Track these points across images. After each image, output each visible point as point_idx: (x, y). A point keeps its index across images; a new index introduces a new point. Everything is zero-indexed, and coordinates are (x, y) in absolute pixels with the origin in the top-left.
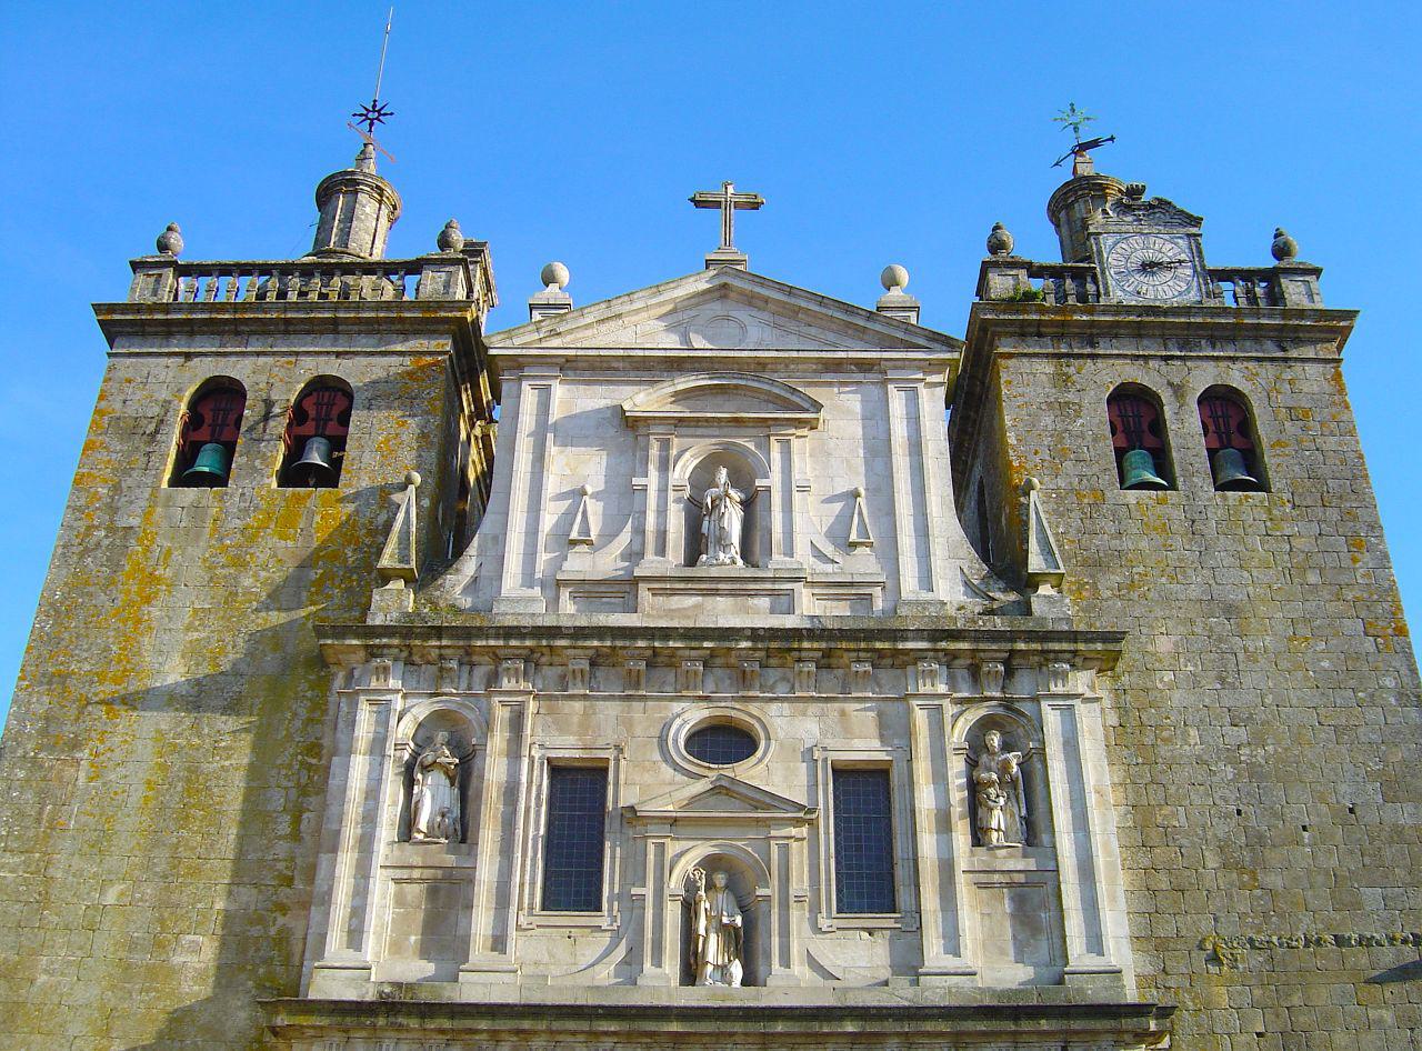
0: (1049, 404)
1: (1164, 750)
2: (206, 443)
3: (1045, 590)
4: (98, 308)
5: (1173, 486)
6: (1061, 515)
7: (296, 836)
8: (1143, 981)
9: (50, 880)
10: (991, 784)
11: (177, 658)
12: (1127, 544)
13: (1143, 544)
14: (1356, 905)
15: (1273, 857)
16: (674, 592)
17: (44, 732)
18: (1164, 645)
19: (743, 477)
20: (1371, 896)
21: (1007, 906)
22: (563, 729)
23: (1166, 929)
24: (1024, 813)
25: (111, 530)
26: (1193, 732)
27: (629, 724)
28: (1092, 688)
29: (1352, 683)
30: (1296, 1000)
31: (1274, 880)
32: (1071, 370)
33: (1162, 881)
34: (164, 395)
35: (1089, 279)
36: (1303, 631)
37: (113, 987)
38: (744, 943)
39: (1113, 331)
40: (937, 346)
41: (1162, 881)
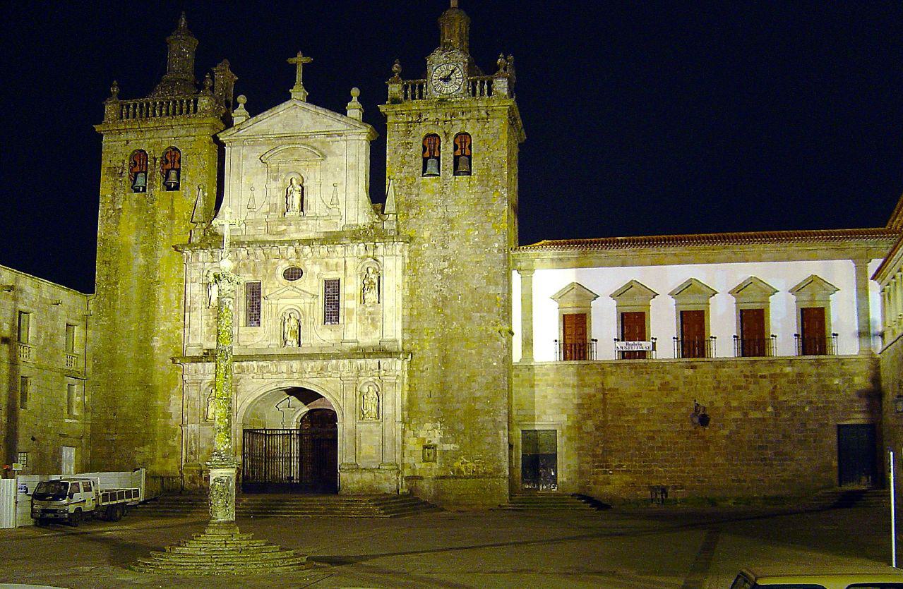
1: (421, 270)
2: (139, 172)
7: (179, 307)
11: (141, 254)
17: (107, 279)
18: (426, 234)
21: (370, 321)
26: (431, 264)
31: (448, 311)
35: (425, 86)
37: (137, 353)
39: (427, 111)
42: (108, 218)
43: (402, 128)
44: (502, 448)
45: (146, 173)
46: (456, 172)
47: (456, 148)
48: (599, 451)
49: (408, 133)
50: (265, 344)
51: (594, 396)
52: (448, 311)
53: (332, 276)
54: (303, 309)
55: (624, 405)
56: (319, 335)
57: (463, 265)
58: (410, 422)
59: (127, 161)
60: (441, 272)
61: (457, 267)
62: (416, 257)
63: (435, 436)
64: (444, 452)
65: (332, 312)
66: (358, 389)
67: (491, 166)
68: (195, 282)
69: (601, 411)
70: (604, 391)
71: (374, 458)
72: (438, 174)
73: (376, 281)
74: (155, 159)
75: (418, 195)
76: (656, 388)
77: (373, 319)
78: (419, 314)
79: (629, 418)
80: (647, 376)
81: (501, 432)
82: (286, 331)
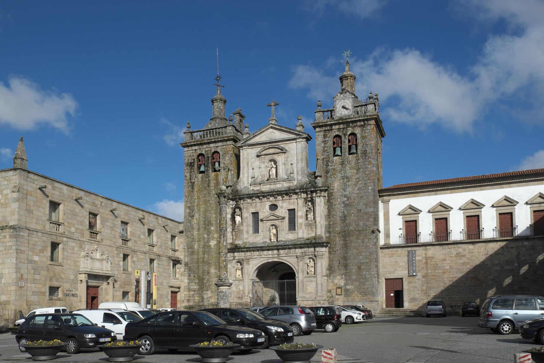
0: (323, 141)
3: (319, 178)
4: (180, 144)
5: (341, 156)
6: (323, 163)
8: (327, 237)
9: (193, 235)
10: (308, 211)
12: (333, 167)
13: (335, 167)
14: (359, 225)
15: (348, 218)
16: (266, 185)
17: (189, 215)
19: (275, 163)
20: (361, 223)
21: (310, 228)
22: (253, 208)
23: (331, 230)
24: (313, 214)
25: (191, 182)
27: (261, 206)
28: (324, 194)
29: (364, 189)
30: (348, 239)
32: (327, 133)
33: (331, 223)
34: (193, 158)
36: (358, 180)
38: (276, 235)
40: (304, 135)
41: (331, 223)
42: (188, 186)
43: (322, 133)
44: (375, 287)
45: (204, 164)
46: (350, 154)
47: (349, 141)
48: (424, 288)
49: (325, 136)
50: (262, 241)
51: (421, 261)
52: (347, 222)
53: (291, 207)
54: (278, 224)
55: (437, 265)
56: (286, 236)
57: (354, 199)
58: (330, 276)
59: (196, 160)
60: (344, 202)
61: (351, 200)
62: (331, 196)
63: (342, 283)
64: (347, 291)
65: (292, 225)
66: (305, 261)
67: (367, 149)
68: (229, 214)
69: (425, 268)
70: (426, 258)
71: (313, 293)
72: (341, 155)
73: (312, 208)
74: (208, 157)
75: (331, 166)
76: (453, 256)
77: (311, 228)
78: (333, 224)
79: (440, 271)
80: (449, 250)
81: (374, 279)
82: (271, 235)
